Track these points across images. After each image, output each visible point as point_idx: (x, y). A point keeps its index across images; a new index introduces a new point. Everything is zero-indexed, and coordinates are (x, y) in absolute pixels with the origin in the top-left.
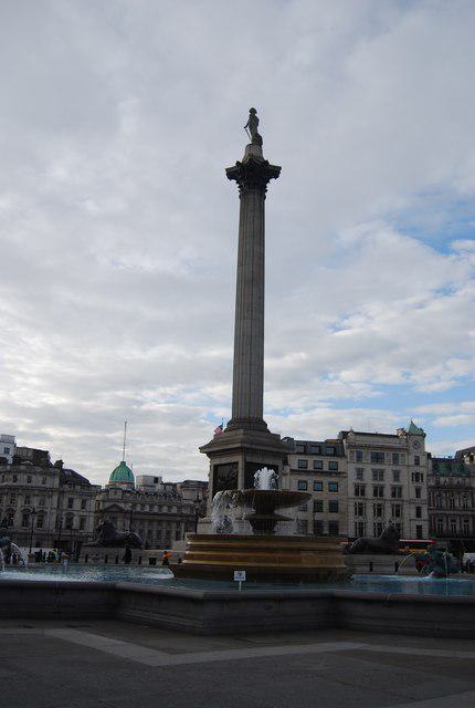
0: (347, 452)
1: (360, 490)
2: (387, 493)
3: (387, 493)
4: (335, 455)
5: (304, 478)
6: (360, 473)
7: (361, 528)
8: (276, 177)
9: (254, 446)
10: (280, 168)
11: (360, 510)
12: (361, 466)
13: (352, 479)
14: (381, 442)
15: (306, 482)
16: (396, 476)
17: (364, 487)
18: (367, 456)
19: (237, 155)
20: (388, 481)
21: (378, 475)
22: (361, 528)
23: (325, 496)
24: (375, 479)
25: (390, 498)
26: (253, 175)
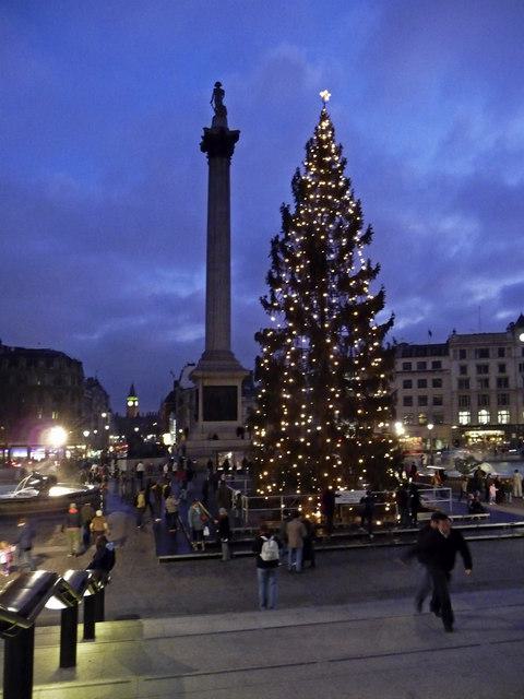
1: (464, 384)
2: (493, 384)
3: (493, 384)
4: (440, 355)
5: (408, 377)
6: (463, 370)
10: (238, 132)
13: (455, 374)
15: (410, 381)
16: (502, 368)
18: (470, 354)
20: (493, 374)
21: (483, 369)
23: (430, 392)
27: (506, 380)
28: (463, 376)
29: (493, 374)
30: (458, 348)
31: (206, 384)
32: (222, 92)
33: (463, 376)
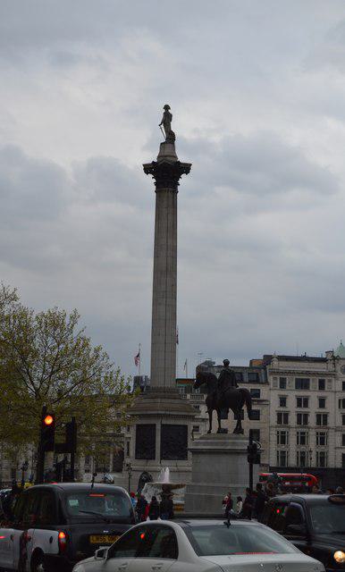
0: (270, 379)
1: (283, 418)
2: (312, 420)
3: (312, 420)
6: (283, 402)
7: (283, 456)
8: (187, 172)
9: (168, 413)
11: (283, 439)
12: (283, 393)
13: (275, 405)
14: (305, 367)
16: (322, 403)
17: (286, 415)
18: (291, 382)
19: (152, 156)
20: (313, 408)
21: (302, 402)
22: (283, 456)
24: (299, 405)
25: (315, 425)
26: (167, 172)
27: (326, 416)
28: (282, 409)
29: (313, 408)
30: (278, 377)
31: (164, 422)
32: (171, 116)
33: (282, 409)
